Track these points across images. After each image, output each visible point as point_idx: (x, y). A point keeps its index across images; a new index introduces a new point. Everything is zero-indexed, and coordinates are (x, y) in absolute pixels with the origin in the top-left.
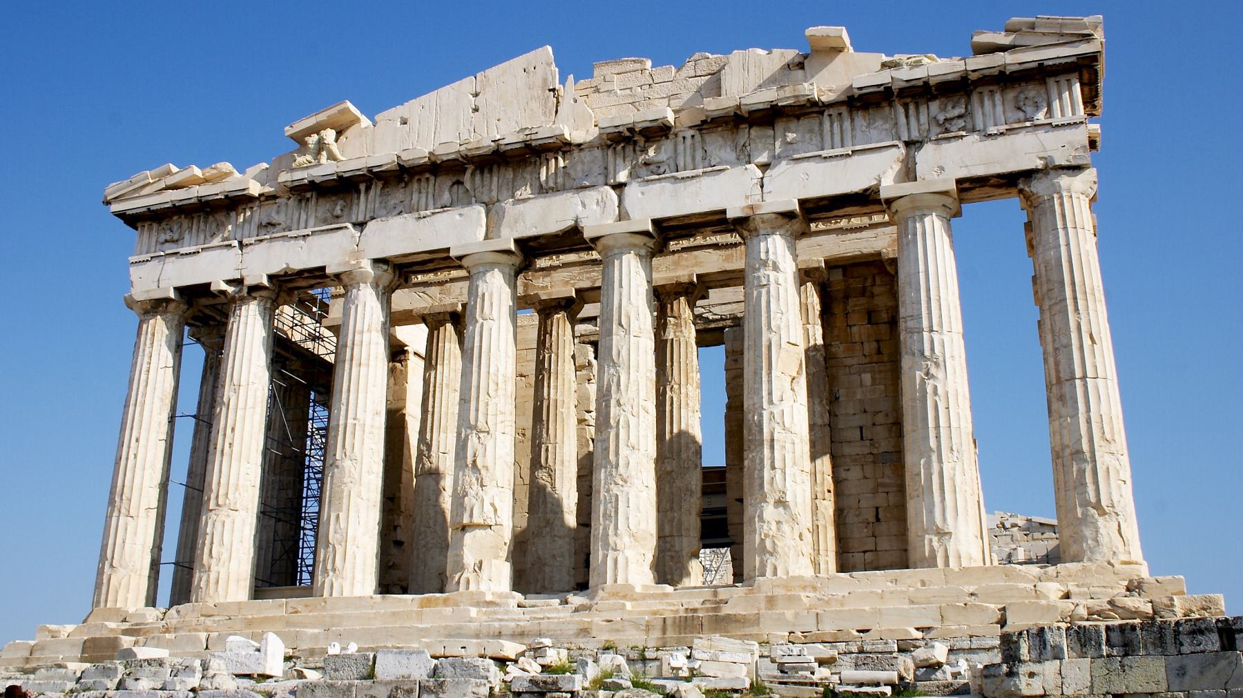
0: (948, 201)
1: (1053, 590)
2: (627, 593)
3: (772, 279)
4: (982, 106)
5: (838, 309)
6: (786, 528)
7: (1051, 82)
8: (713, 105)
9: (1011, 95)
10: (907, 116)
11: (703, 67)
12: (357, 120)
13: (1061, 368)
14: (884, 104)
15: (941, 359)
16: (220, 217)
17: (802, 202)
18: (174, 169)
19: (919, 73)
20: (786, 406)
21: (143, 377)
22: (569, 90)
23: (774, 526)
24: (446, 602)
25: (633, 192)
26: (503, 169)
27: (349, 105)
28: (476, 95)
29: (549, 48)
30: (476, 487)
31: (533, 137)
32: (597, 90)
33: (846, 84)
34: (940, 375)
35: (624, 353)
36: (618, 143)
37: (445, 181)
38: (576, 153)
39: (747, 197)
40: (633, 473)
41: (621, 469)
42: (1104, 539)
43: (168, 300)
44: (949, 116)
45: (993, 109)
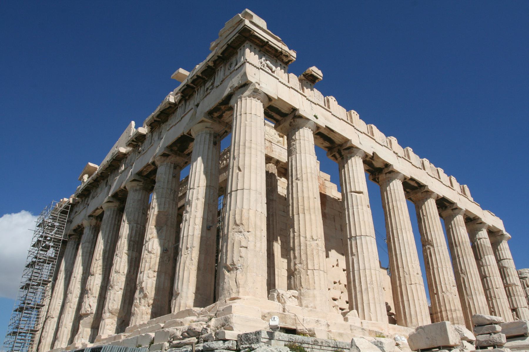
6: (143, 301)
37: (105, 181)
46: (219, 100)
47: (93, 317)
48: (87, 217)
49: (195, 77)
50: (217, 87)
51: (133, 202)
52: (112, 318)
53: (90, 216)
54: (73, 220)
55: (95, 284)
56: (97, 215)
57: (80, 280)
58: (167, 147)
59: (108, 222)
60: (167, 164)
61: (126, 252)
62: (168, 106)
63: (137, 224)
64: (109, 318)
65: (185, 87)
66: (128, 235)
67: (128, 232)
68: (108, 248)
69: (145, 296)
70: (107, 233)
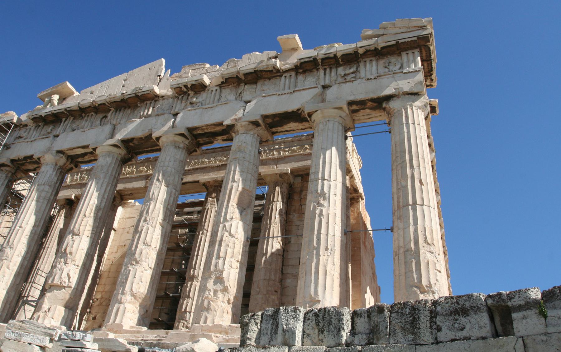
2: (118, 329)
4: (365, 66)
5: (296, 197)
6: (220, 295)
9: (382, 62)
10: (325, 74)
12: (73, 93)
14: (315, 70)
15: (327, 195)
17: (265, 117)
20: (234, 223)
23: (212, 293)
26: (126, 110)
27: (68, 83)
30: (62, 264)
31: (140, 91)
34: (325, 203)
35: (156, 193)
36: (180, 95)
37: (100, 116)
40: (143, 259)
41: (137, 256)
44: (347, 72)
45: (370, 68)
46: (374, 96)
47: (70, 292)
48: (55, 152)
49: (332, 55)
50: (368, 79)
51: (175, 161)
52: (134, 303)
53: (59, 152)
54: (12, 146)
55: (80, 248)
56: (70, 154)
57: (29, 234)
58: (262, 116)
59: (108, 171)
60: (253, 134)
61: (161, 221)
62: (271, 69)
63: (176, 190)
64: (130, 302)
65: (311, 59)
66: (165, 200)
67: (165, 196)
68: (103, 205)
69: (225, 290)
70: (105, 185)
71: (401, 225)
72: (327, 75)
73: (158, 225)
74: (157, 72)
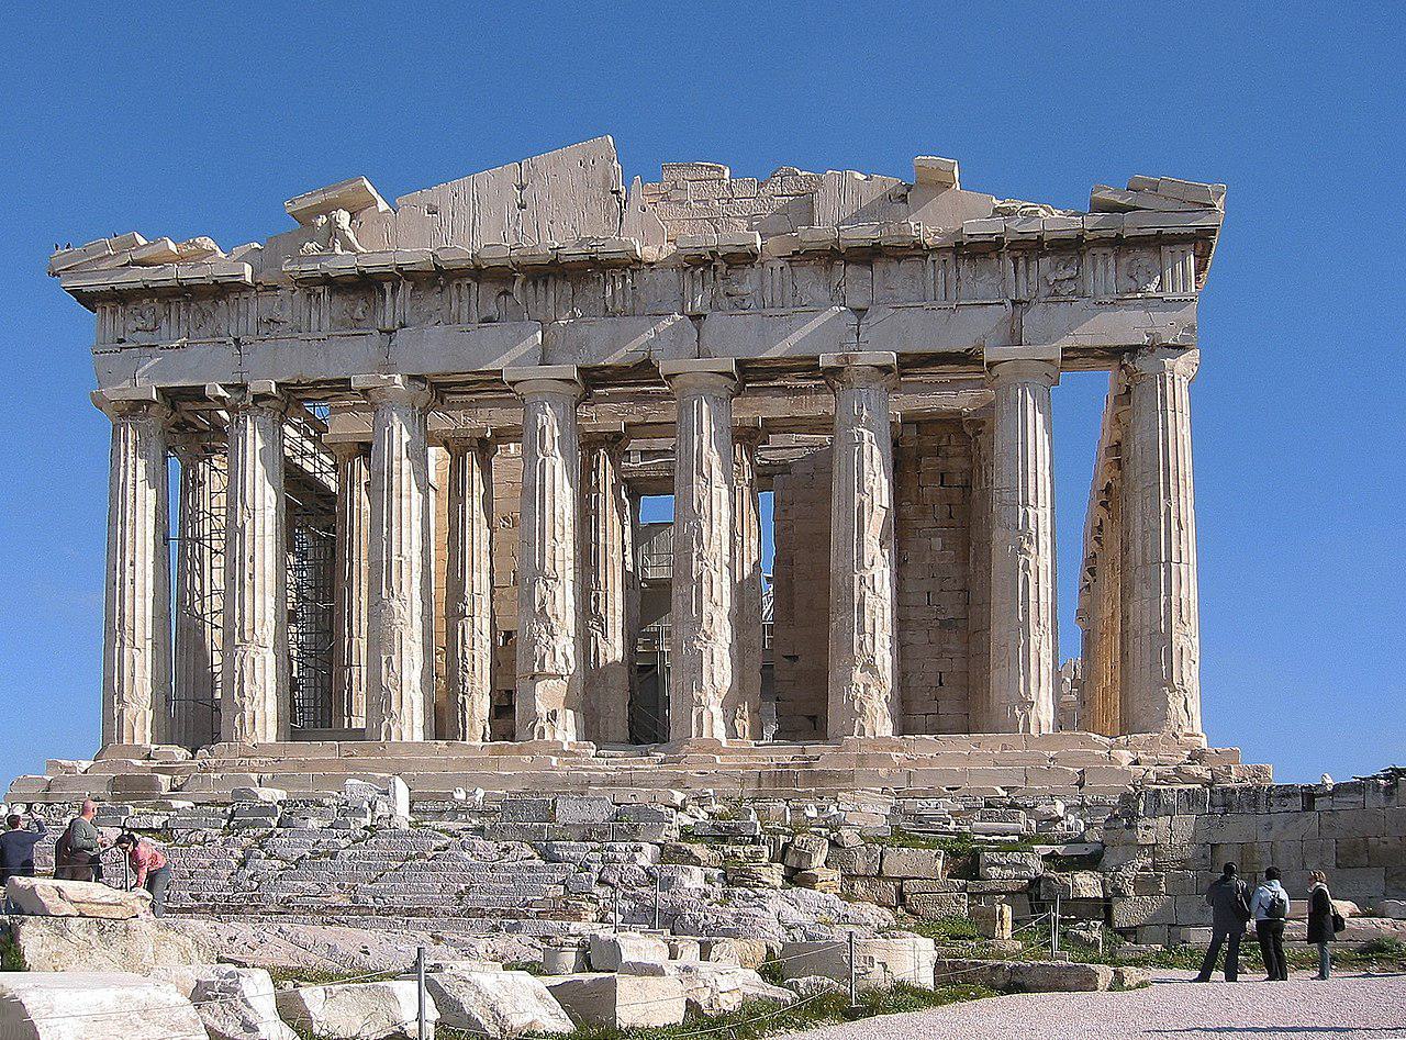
0: (1051, 369)
1: (1125, 757)
3: (866, 437)
6: (873, 690)
7: (1166, 250)
8: (808, 236)
11: (791, 186)
13: (1148, 551)
14: (993, 255)
16: (206, 305)
18: (142, 241)
19: (1033, 228)
20: (876, 570)
21: (130, 491)
22: (639, 194)
23: (862, 690)
24: (520, 750)
25: (715, 322)
28: (522, 188)
29: (610, 139)
32: (666, 198)
33: (952, 227)
34: (1033, 550)
35: (705, 503)
37: (489, 291)
38: (647, 273)
39: (842, 345)
41: (705, 626)
42: (1172, 714)
43: (150, 402)
71: (1147, 593)
72: (1022, 277)
73: (724, 567)
74: (607, 178)
